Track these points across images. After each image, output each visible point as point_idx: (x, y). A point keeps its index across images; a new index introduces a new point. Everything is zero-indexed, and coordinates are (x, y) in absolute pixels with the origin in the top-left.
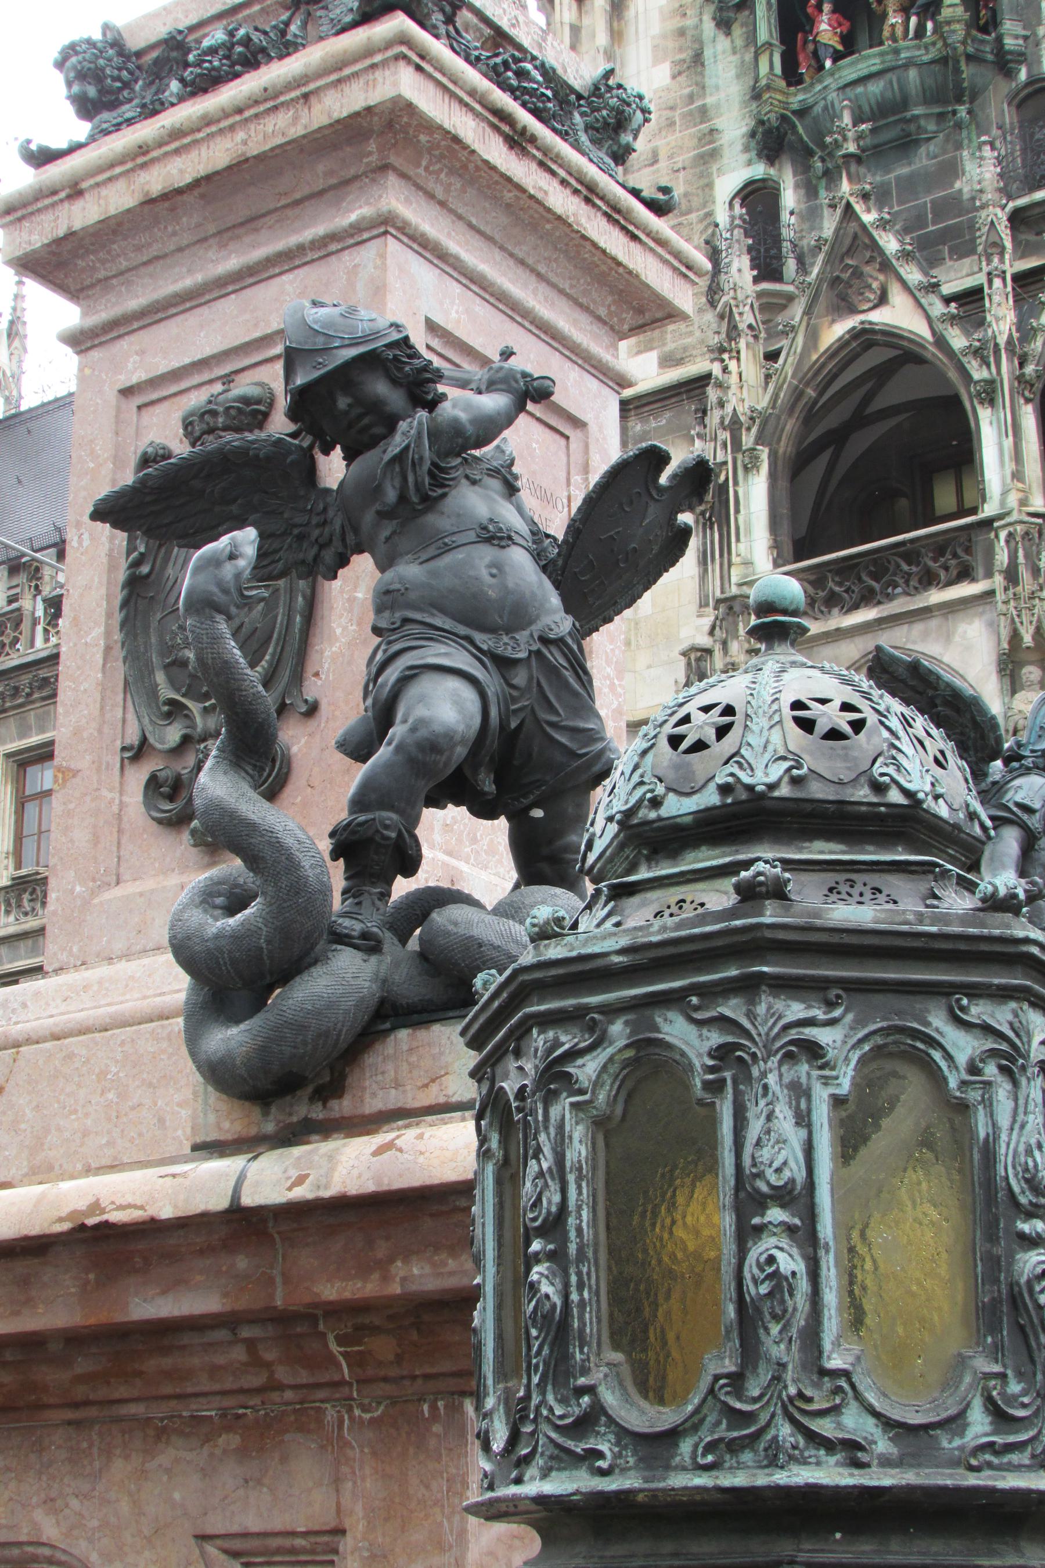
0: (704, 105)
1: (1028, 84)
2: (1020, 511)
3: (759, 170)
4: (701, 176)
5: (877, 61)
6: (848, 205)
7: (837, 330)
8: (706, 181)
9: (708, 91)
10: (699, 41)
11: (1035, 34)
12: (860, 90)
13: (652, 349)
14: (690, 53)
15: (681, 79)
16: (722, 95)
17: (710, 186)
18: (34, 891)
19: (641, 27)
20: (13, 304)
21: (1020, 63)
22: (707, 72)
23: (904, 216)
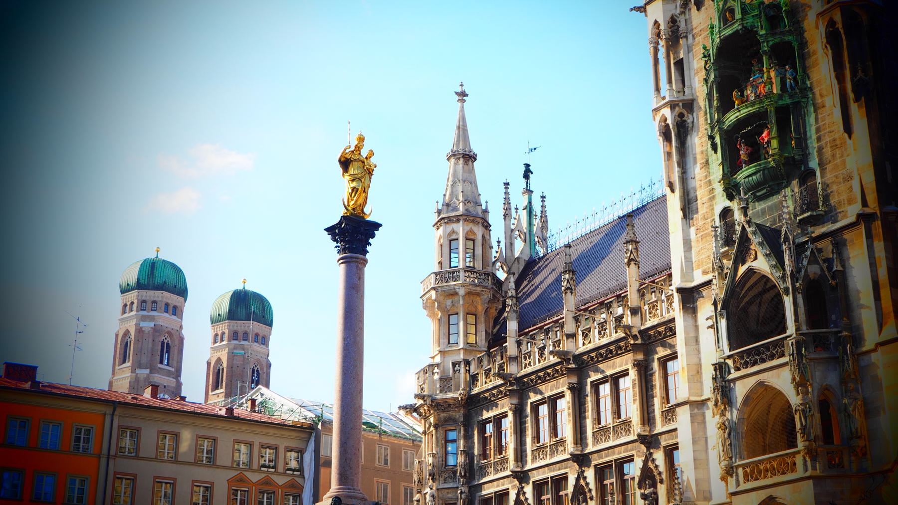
0: (710, 180)
1: (805, 171)
2: (796, 333)
3: (728, 203)
4: (711, 206)
5: (754, 169)
6: (743, 226)
7: (742, 270)
8: (712, 207)
9: (711, 174)
10: (707, 155)
11: (806, 153)
12: (750, 178)
13: (700, 268)
14: (705, 160)
15: (703, 170)
16: (715, 176)
17: (713, 209)
18: (543, 451)
19: (690, 150)
20: (541, 210)
21: (801, 164)
22: (710, 168)
23: (770, 220)
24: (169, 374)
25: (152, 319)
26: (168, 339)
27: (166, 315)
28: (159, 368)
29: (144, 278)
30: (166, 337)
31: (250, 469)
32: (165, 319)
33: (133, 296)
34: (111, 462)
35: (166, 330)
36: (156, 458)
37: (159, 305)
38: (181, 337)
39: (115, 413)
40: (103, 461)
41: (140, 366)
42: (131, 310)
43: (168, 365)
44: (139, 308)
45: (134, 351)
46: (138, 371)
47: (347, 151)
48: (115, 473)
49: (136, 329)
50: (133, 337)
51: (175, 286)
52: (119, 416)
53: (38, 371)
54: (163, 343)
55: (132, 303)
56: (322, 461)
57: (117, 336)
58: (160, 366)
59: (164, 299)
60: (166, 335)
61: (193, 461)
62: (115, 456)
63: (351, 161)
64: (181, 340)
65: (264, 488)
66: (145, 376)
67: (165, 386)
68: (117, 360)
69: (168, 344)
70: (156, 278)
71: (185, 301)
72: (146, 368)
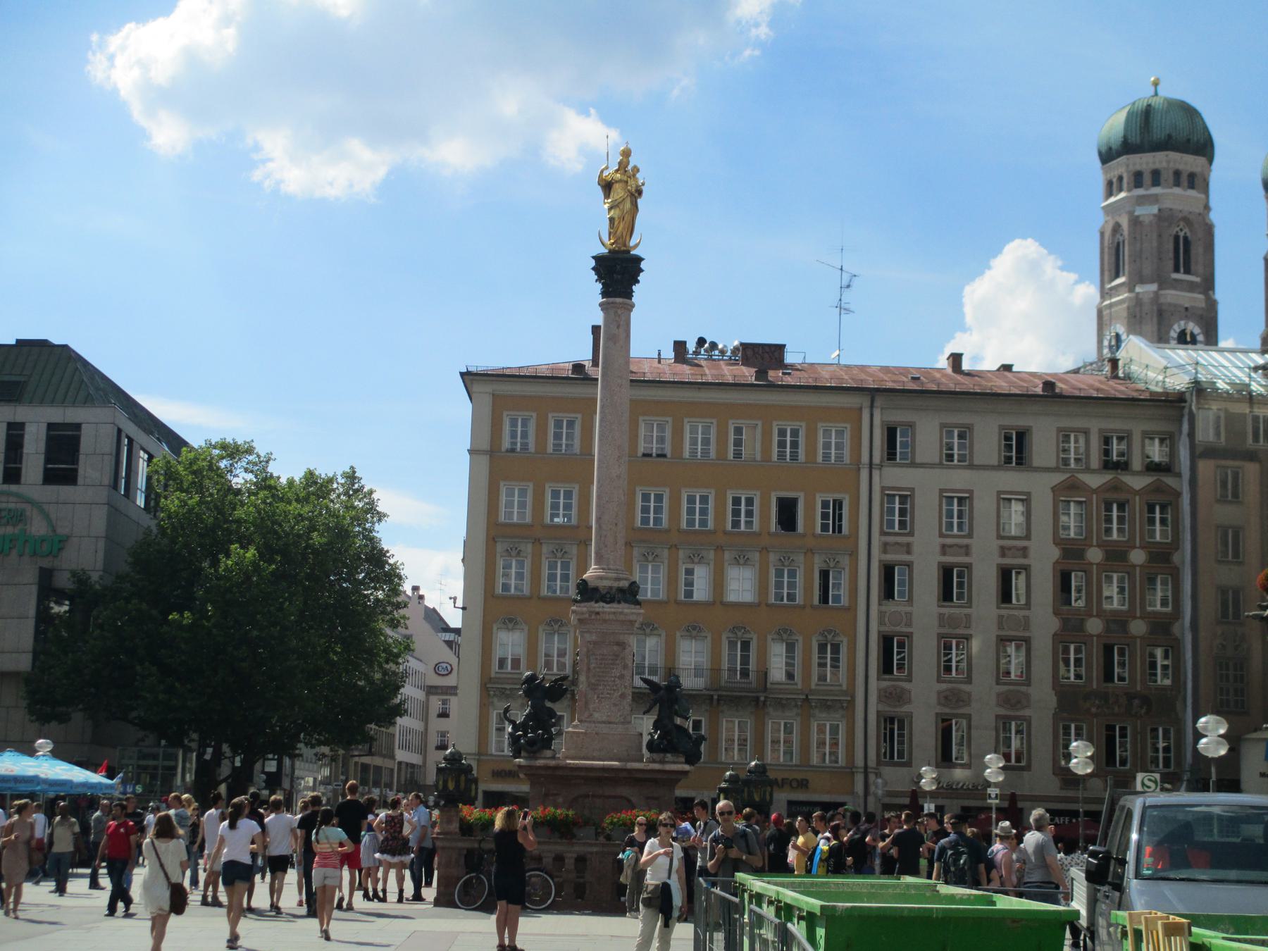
24: (1192, 287)
25: (1154, 199)
26: (1186, 230)
27: (1177, 190)
28: (1176, 280)
29: (1134, 135)
30: (1181, 226)
31: (1088, 470)
32: (1176, 198)
33: (1123, 165)
34: (876, 473)
35: (1180, 215)
36: (941, 463)
37: (1164, 176)
38: (1207, 224)
39: (875, 404)
40: (864, 474)
41: (1142, 281)
42: (1120, 190)
43: (1187, 271)
44: (1132, 184)
45: (1130, 256)
46: (1138, 289)
47: (606, 173)
48: (883, 489)
49: (1130, 221)
50: (1126, 233)
51: (1189, 140)
52: (882, 409)
53: (788, 348)
54: (1177, 238)
55: (1120, 178)
56: (1197, 453)
57: (1102, 234)
58: (1175, 276)
59: (1172, 165)
60: (1182, 224)
61: (996, 463)
62: (881, 466)
63: (613, 183)
64: (1209, 230)
65: (1108, 496)
66: (1152, 295)
67: (1187, 309)
68: (1106, 273)
69: (1186, 238)
70: (1155, 131)
71: (1211, 161)
72: (1152, 282)
